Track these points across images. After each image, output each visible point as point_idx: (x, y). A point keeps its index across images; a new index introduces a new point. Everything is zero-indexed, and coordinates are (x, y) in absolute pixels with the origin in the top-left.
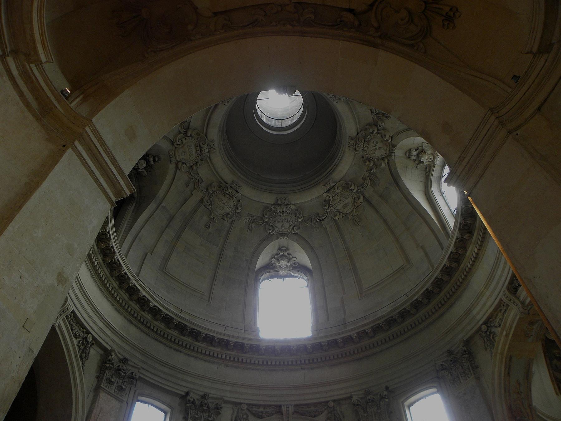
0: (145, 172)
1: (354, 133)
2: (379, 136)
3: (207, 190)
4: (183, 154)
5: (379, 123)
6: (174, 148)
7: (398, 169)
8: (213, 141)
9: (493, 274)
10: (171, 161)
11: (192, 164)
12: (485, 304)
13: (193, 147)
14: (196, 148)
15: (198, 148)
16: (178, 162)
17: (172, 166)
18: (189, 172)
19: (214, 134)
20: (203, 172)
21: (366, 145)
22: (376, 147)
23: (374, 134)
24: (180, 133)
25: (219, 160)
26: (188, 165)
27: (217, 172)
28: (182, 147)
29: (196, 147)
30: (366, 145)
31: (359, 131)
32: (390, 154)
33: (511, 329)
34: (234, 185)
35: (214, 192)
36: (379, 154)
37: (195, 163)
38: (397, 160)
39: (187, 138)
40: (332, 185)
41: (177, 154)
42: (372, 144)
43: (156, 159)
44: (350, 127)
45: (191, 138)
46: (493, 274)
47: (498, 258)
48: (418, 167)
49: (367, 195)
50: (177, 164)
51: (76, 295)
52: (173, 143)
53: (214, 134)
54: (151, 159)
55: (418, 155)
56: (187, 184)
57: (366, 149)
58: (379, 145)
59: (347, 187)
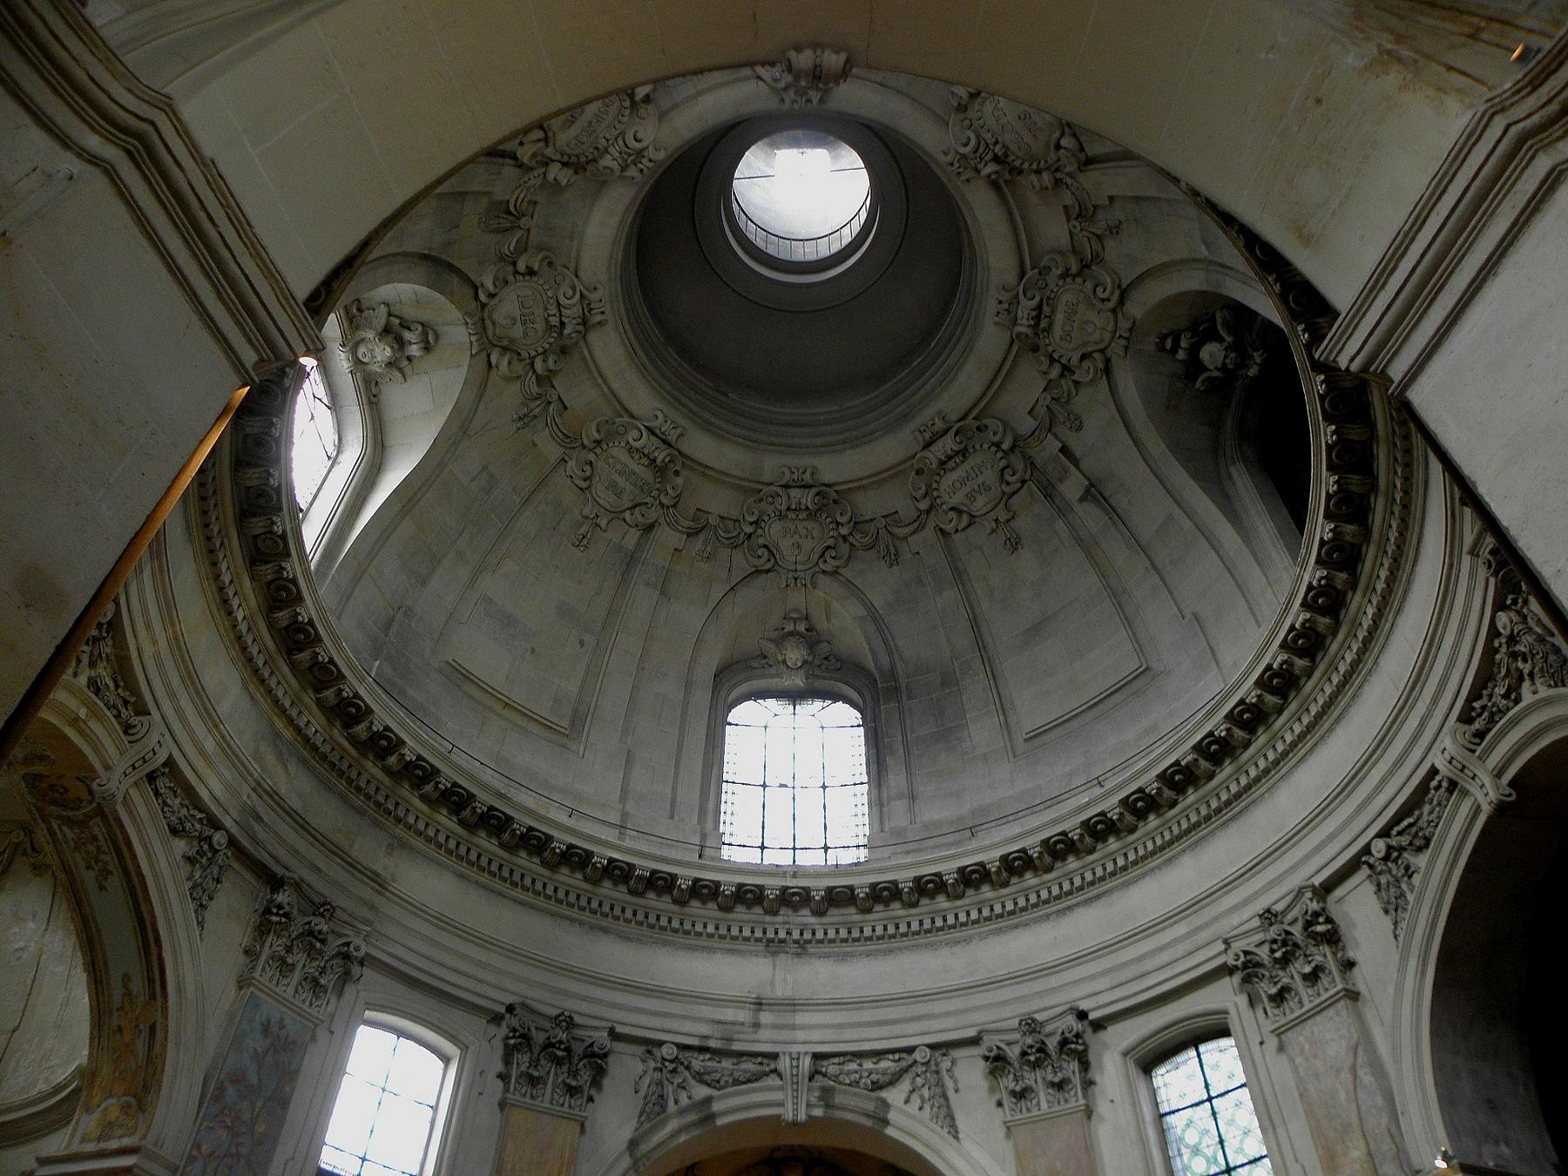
0: (1219, 319)
1: (594, 338)
2: (524, 354)
3: (1058, 182)
4: (1090, 329)
5: (535, 390)
6: (1109, 352)
7: (442, 298)
8: (996, 324)
9: (193, 684)
10: (1131, 330)
11: (1079, 280)
12: (149, 626)
13: (1058, 330)
14: (1051, 325)
15: (1044, 324)
16: (1114, 311)
17: (1137, 307)
18: (1097, 258)
19: (990, 341)
20: (1054, 230)
21: (554, 321)
22: (524, 323)
23: (540, 350)
24: (1077, 383)
25: (996, 256)
26: (1089, 285)
27: (1012, 221)
28: (1086, 344)
29: (1049, 329)
30: (554, 321)
31: (582, 343)
32: (481, 322)
33: (82, 733)
34: (969, 174)
35: (1038, 172)
36: (507, 308)
37: (1069, 280)
38: (455, 313)
39: (1064, 361)
40: (632, 172)
41: (1107, 336)
42: (540, 326)
43: (1168, 345)
44: (609, 349)
45: (1056, 356)
46: (193, 684)
47: (216, 726)
48: (383, 309)
49: (509, 171)
50: (1121, 302)
51: (1451, 662)
52: (1108, 370)
53: (990, 341)
54: (1181, 355)
55: (401, 343)
56: (1115, 230)
57: (553, 310)
58: (517, 332)
59: (577, 165)
